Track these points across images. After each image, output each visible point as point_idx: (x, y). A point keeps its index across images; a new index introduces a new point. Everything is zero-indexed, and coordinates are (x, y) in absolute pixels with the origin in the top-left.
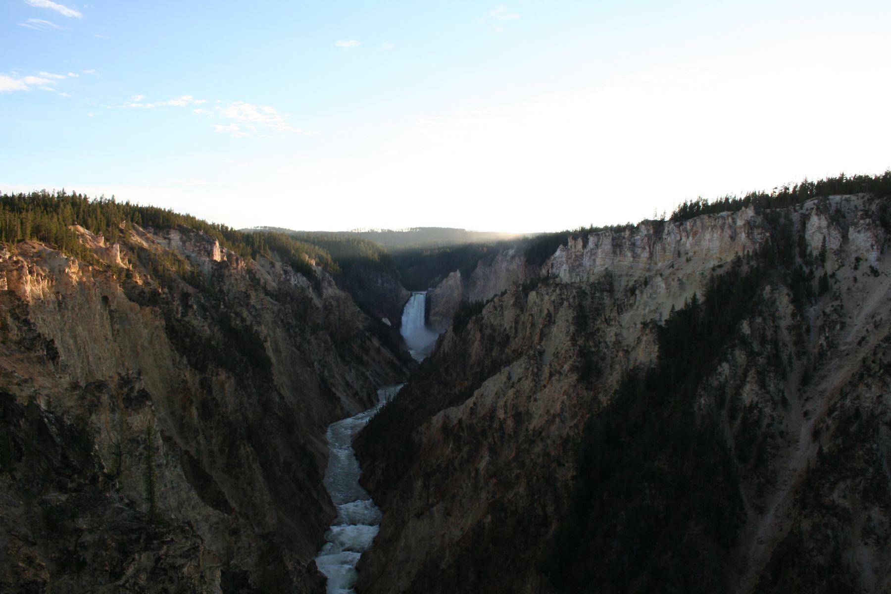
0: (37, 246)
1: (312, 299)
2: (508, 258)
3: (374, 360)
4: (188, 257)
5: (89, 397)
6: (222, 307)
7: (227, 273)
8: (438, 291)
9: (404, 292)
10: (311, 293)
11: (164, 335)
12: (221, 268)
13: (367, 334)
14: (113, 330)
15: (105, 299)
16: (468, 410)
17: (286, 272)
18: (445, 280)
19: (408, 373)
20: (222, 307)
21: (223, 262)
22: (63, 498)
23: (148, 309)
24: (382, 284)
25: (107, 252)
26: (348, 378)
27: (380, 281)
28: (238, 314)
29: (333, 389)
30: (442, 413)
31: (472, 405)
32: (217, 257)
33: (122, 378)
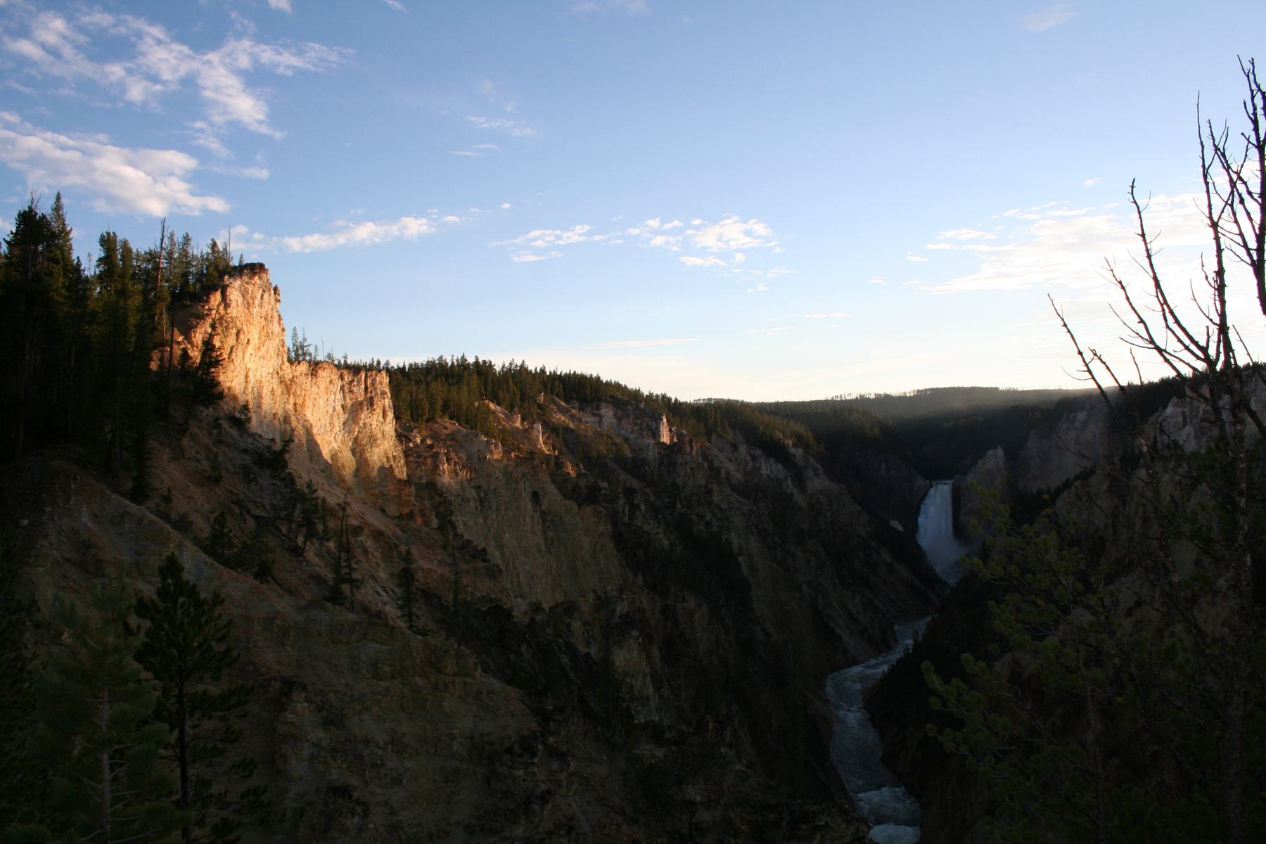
0: (449, 426)
1: (792, 495)
2: (1078, 424)
4: (627, 440)
6: (679, 506)
7: (680, 461)
8: (971, 479)
10: (790, 487)
11: (610, 545)
14: (546, 539)
15: (536, 497)
17: (754, 458)
18: (980, 463)
20: (679, 506)
21: (673, 445)
22: (660, 753)
25: (526, 432)
27: (883, 466)
28: (700, 517)
29: (832, 625)
32: (665, 438)
33: (599, 598)
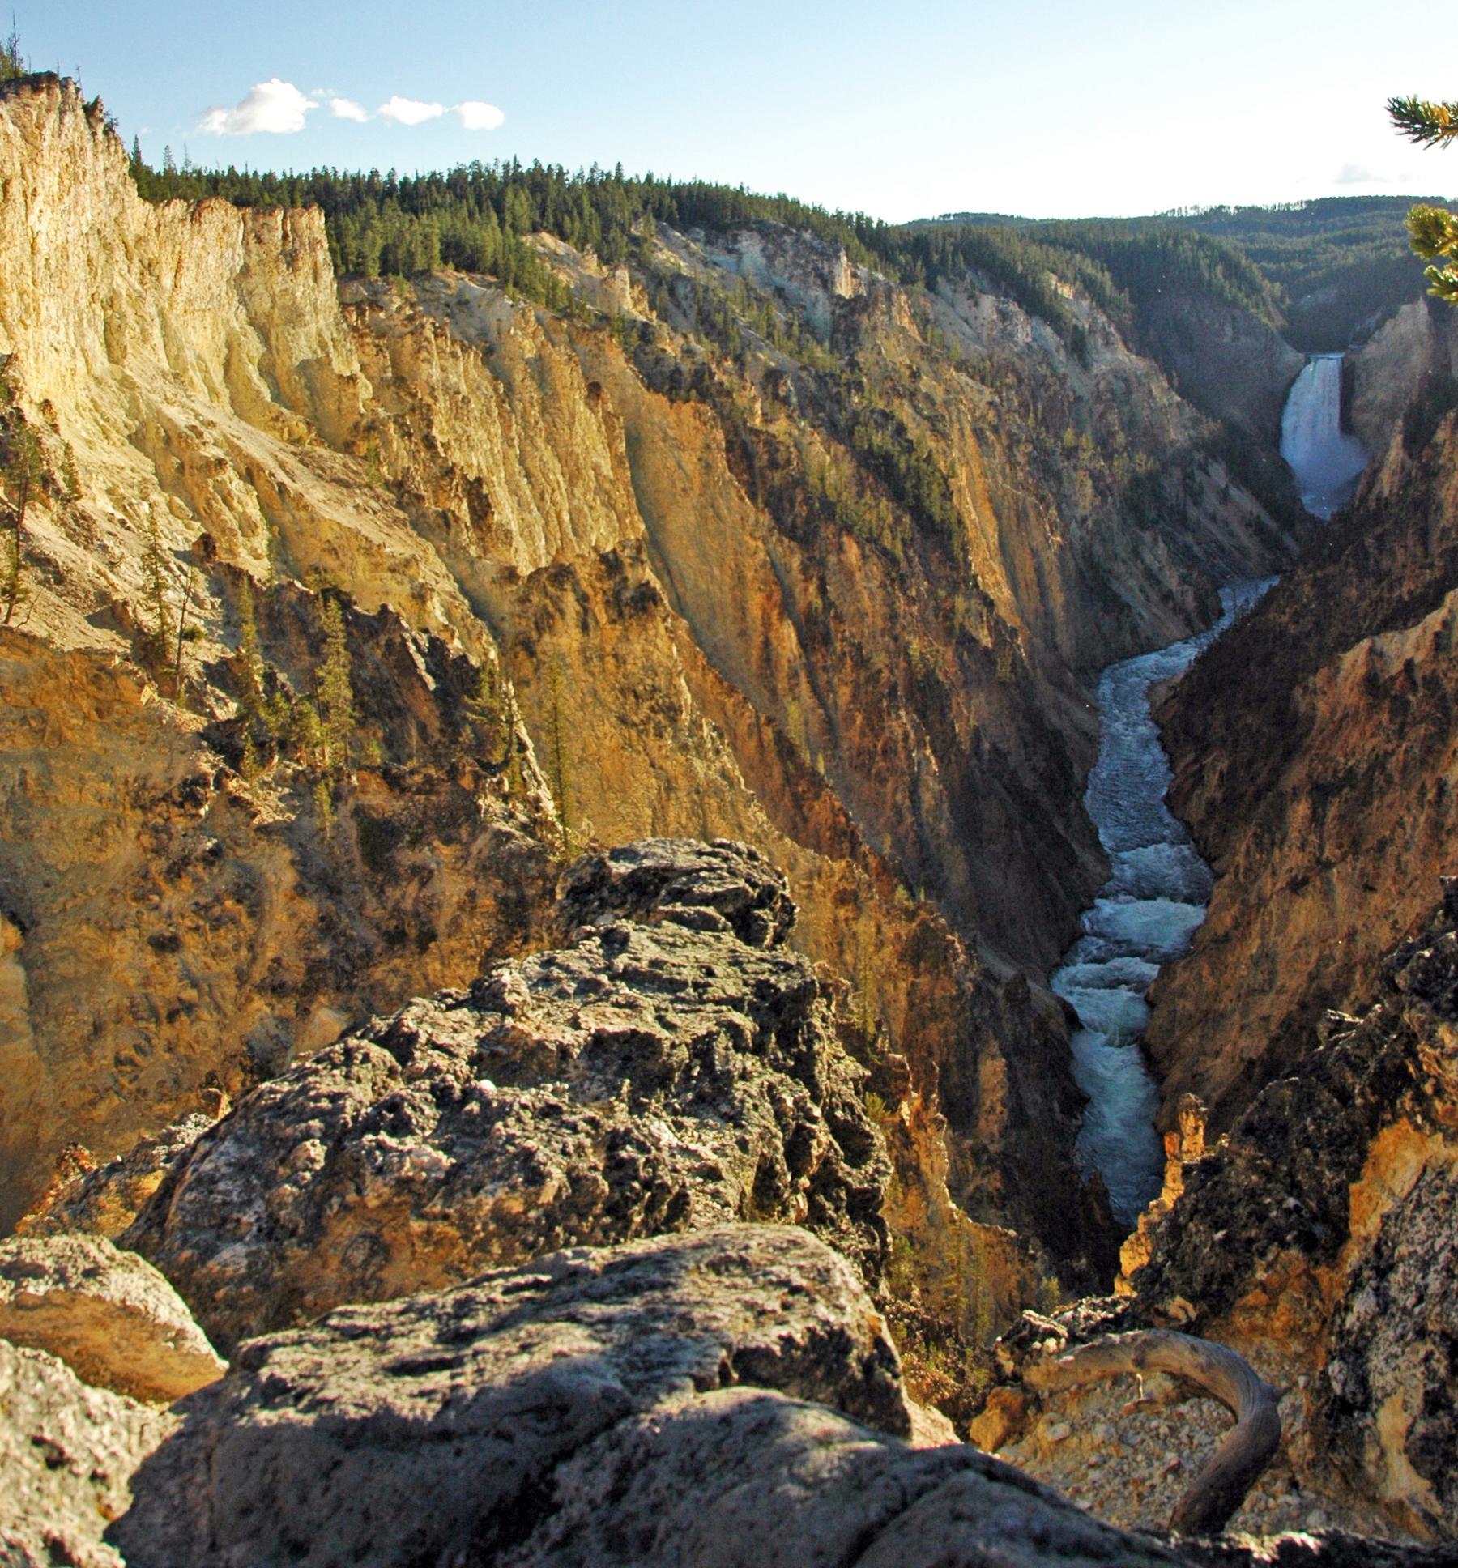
3: (1213, 519)
4: (779, 292)
5: (535, 598)
7: (865, 322)
9: (1290, 355)
12: (853, 311)
13: (1198, 456)
16: (1429, 637)
17: (1004, 316)
18: (1389, 324)
19: (1295, 549)
21: (857, 298)
23: (687, 409)
24: (1235, 338)
26: (1148, 558)
27: (1229, 330)
29: (1115, 585)
30: (1365, 643)
31: (1438, 628)
32: (845, 288)
